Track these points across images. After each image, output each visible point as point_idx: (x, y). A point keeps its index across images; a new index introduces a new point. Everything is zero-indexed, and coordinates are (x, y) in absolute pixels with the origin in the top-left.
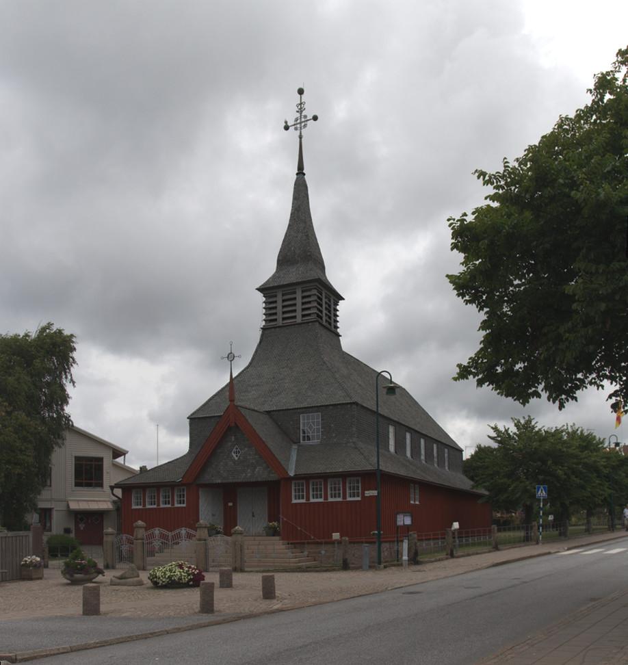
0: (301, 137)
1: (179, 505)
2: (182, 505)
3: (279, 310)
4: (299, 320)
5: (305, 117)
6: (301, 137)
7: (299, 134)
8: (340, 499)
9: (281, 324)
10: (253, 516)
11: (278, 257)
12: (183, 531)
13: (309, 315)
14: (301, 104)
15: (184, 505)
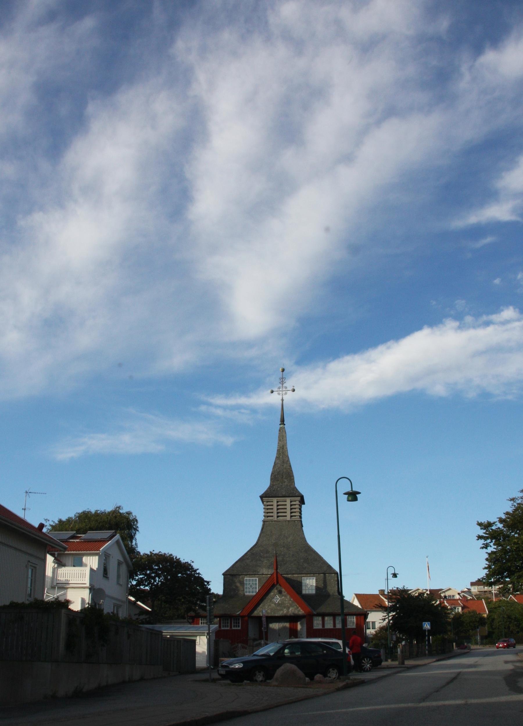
0: (283, 400)
1: (235, 628)
2: (238, 628)
3: (275, 510)
4: (288, 518)
5: (286, 388)
6: (283, 400)
7: (281, 398)
8: (229, 628)
9: (276, 519)
10: (279, 635)
11: (271, 476)
12: (240, 645)
13: (295, 516)
14: (283, 378)
15: (240, 628)
